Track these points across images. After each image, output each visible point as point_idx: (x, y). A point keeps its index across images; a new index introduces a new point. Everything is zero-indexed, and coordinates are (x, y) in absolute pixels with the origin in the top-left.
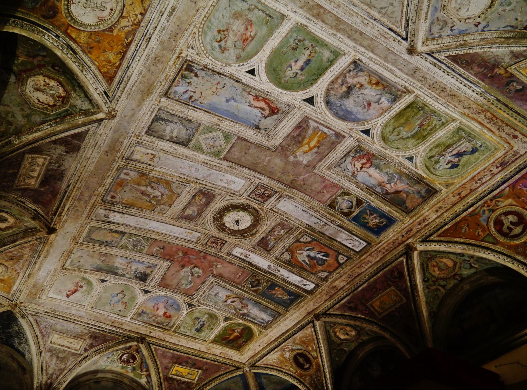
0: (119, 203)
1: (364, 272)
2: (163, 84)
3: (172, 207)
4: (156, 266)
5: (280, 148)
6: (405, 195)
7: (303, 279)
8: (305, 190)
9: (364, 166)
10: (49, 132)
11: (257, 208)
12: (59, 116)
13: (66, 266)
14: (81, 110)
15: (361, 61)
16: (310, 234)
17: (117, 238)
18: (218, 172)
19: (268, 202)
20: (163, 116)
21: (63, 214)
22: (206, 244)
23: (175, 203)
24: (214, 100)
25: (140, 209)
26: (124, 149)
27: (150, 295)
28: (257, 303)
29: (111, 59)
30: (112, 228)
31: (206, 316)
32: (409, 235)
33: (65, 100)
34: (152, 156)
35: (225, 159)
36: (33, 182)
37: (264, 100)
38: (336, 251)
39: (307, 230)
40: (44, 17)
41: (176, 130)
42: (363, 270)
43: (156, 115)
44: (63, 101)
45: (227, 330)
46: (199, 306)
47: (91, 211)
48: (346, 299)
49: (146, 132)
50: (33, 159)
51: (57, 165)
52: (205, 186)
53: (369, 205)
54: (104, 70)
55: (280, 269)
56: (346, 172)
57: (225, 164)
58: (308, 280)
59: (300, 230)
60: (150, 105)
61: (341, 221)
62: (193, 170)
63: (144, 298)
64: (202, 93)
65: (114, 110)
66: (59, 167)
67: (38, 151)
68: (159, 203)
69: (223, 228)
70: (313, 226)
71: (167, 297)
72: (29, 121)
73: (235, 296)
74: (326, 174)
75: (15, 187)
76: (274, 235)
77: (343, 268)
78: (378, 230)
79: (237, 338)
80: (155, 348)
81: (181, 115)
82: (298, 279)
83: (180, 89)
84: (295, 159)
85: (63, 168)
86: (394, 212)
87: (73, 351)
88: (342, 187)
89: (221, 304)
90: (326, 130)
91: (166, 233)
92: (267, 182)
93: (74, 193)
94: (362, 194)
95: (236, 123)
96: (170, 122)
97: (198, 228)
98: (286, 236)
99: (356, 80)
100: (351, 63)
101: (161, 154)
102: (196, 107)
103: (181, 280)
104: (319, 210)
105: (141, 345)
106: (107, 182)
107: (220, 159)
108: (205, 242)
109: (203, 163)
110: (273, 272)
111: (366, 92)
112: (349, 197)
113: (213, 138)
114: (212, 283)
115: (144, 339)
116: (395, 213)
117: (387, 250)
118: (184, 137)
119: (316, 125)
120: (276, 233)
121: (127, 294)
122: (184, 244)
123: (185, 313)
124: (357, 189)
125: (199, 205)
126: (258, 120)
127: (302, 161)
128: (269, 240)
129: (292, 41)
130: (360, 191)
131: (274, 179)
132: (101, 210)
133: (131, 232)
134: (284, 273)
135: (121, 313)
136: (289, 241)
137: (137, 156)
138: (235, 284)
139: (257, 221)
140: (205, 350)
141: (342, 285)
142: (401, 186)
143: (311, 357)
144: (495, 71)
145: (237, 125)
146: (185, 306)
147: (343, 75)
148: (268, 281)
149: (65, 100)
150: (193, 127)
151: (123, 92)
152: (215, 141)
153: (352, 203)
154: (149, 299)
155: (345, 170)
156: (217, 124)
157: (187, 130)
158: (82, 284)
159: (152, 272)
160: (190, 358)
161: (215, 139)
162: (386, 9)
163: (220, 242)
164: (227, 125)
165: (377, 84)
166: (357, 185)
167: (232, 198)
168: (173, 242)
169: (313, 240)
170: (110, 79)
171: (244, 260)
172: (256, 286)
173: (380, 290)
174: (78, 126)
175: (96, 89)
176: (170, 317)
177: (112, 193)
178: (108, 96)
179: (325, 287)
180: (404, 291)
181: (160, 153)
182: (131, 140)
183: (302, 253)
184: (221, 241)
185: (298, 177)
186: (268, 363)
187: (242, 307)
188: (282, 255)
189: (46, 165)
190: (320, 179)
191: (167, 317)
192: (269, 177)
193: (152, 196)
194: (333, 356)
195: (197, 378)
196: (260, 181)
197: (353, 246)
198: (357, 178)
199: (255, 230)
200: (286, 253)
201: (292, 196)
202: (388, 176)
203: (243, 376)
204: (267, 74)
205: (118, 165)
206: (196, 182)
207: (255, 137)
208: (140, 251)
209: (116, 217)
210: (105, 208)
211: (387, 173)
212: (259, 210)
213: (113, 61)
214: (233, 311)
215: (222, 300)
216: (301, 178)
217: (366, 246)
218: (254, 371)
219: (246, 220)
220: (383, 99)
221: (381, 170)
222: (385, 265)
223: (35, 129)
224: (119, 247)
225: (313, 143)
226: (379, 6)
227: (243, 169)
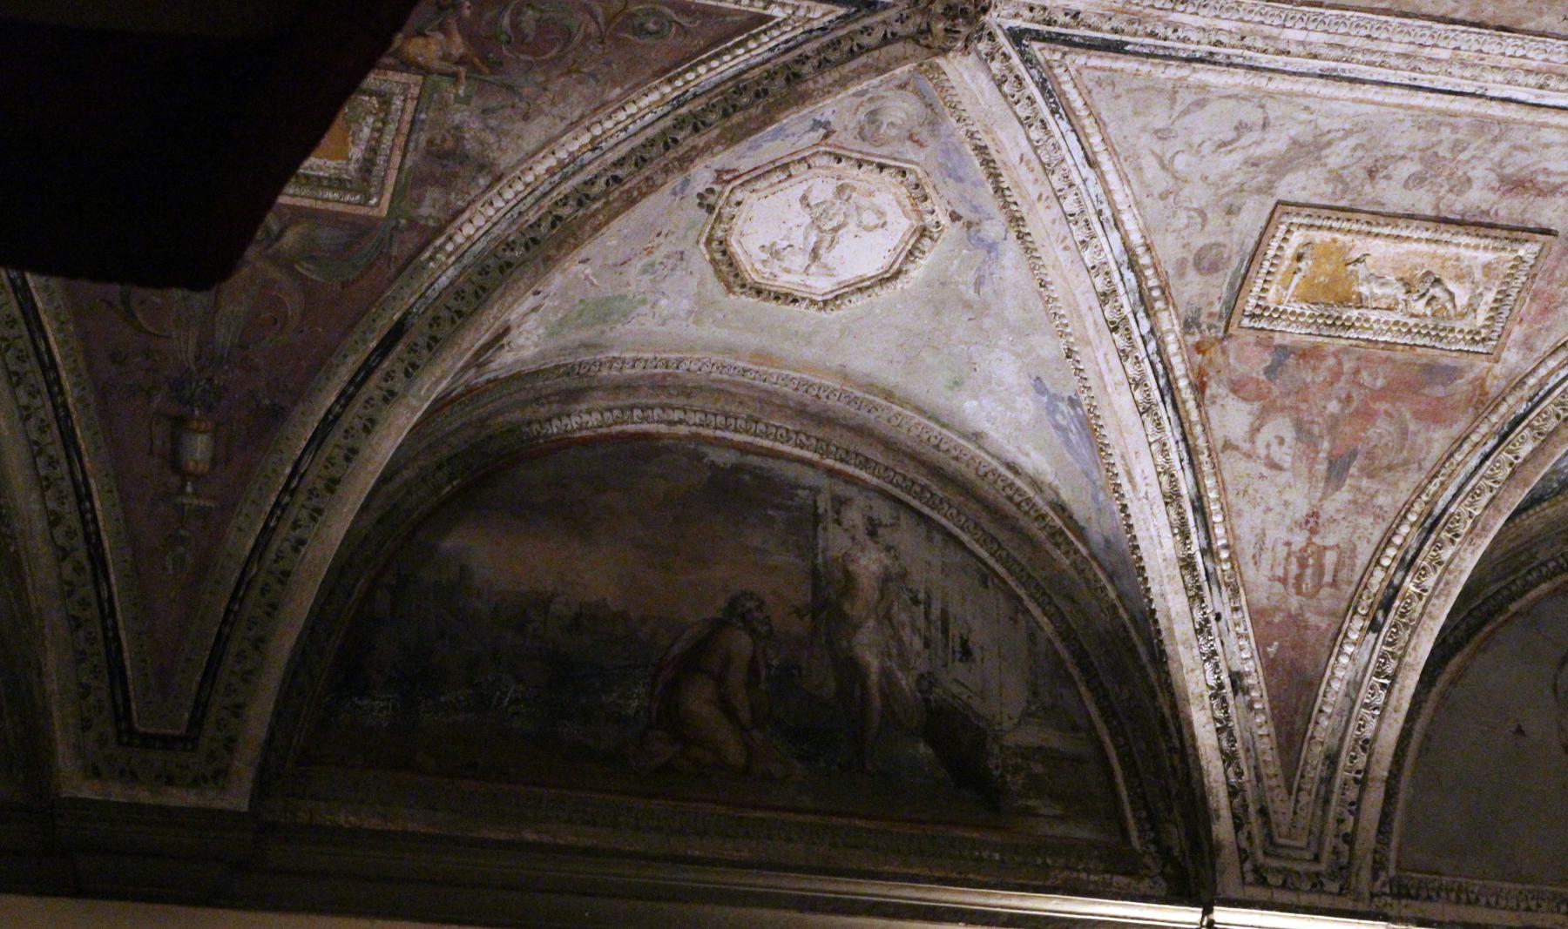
144: (458, 39)
162: (1178, 108)
226: (1215, 107)
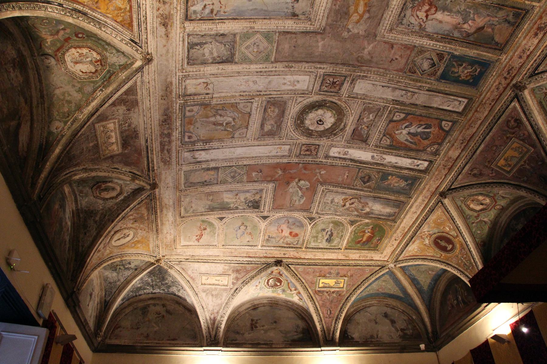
0: (198, 141)
1: (475, 132)
2: (179, 8)
3: (249, 128)
4: (261, 190)
5: (328, 27)
6: (490, 30)
7: (413, 160)
8: (376, 63)
9: (429, 13)
10: (102, 97)
11: (334, 100)
12: (105, 79)
13: (182, 215)
14: (120, 66)
16: (402, 110)
17: (213, 175)
18: (276, 77)
19: (343, 90)
20: (196, 40)
21: (155, 168)
22: (300, 154)
23: (250, 123)
24: (236, 4)
25: (220, 140)
26: (176, 88)
27: (269, 220)
29: (121, 6)
30: (203, 167)
31: (331, 225)
32: (512, 73)
33: (102, 62)
34: (205, 85)
35: (276, 61)
36: (115, 147)
38: (437, 119)
39: (396, 106)
41: (215, 50)
42: (474, 130)
43: (188, 43)
44: (101, 64)
45: (357, 233)
46: (320, 217)
47: (177, 157)
48: (467, 167)
49: (188, 63)
50: (104, 127)
51: (127, 125)
52: (270, 96)
53: (453, 56)
54: (119, 19)
55: (384, 156)
56: (411, 27)
57: (280, 67)
58: (419, 159)
59: (389, 109)
60: (178, 35)
61: (428, 84)
62: (251, 84)
63: (265, 224)
64: (220, 2)
65: (148, 54)
66: (129, 126)
67: (103, 118)
68: (235, 129)
69: (309, 133)
70: (401, 99)
71: (286, 217)
72: (83, 93)
73: (351, 197)
74: (390, 38)
76: (365, 123)
78: (474, 81)
79: (370, 239)
80: (295, 268)
81: (212, 33)
82: (409, 161)
84: (350, 33)
85: (133, 126)
86: (485, 54)
87: (223, 287)
88: (415, 46)
89: (341, 210)
91: (255, 155)
92: (331, 69)
93: (154, 145)
94: (440, 46)
95: (270, 19)
96: (205, 43)
97: (284, 140)
98: (376, 120)
101: (213, 79)
102: (222, 19)
104: (400, 80)
105: (280, 268)
106: (178, 125)
107: (272, 62)
108: (298, 152)
109: (257, 72)
110: (379, 162)
112: (427, 55)
113: (255, 44)
114: (323, 191)
115: (281, 261)
116: (487, 55)
117: (493, 100)
118: (226, 53)
120: (365, 120)
122: (278, 161)
123: (309, 227)
124: (432, 43)
125: (275, 117)
126: (291, 7)
127: (359, 33)
128: (361, 129)
130: (436, 43)
131: (338, 64)
132: (185, 153)
133: (223, 165)
134: (391, 159)
135: (251, 244)
136: (382, 124)
137: (191, 90)
138: (346, 186)
139: (340, 113)
140: (343, 258)
141: (457, 153)
142: (480, 21)
143: (451, 237)
145: (272, 20)
149: (102, 62)
150: (229, 40)
151: (147, 33)
152: (258, 46)
153: (432, 59)
154: (270, 224)
155: (409, 25)
156: (251, 28)
157: (225, 45)
158: (204, 227)
159: (261, 197)
161: (257, 44)
163: (313, 148)
164: (261, 26)
166: (429, 37)
167: (303, 99)
168: (268, 162)
170: (130, 26)
171: (345, 159)
172: (368, 181)
173: (500, 146)
174: (125, 82)
175: (122, 40)
176: (296, 235)
177: (187, 134)
178: (136, 43)
179: (439, 161)
180: (527, 139)
181: (211, 79)
182: (177, 77)
183: (401, 133)
185: (361, 53)
186: (410, 254)
188: (381, 141)
189: (117, 128)
190: (386, 46)
191: (294, 236)
192: (331, 63)
193: (225, 124)
194: (474, 230)
195: (345, 285)
196: (324, 71)
197: (453, 107)
198: (427, 30)
199: (343, 124)
200: (384, 137)
201: (365, 75)
202: (462, 15)
203: (391, 273)
205: (178, 105)
206: (260, 95)
207: (296, 25)
209: (202, 156)
210: (188, 150)
211: (458, 12)
212: (337, 101)
213: (122, 7)
214: (356, 213)
215: (340, 205)
216: (366, 51)
217: (468, 103)
218: (399, 265)
219: (329, 119)
221: (450, 11)
222: (497, 117)
223: (91, 99)
224: (219, 183)
225: (361, 9)
227: (300, 64)
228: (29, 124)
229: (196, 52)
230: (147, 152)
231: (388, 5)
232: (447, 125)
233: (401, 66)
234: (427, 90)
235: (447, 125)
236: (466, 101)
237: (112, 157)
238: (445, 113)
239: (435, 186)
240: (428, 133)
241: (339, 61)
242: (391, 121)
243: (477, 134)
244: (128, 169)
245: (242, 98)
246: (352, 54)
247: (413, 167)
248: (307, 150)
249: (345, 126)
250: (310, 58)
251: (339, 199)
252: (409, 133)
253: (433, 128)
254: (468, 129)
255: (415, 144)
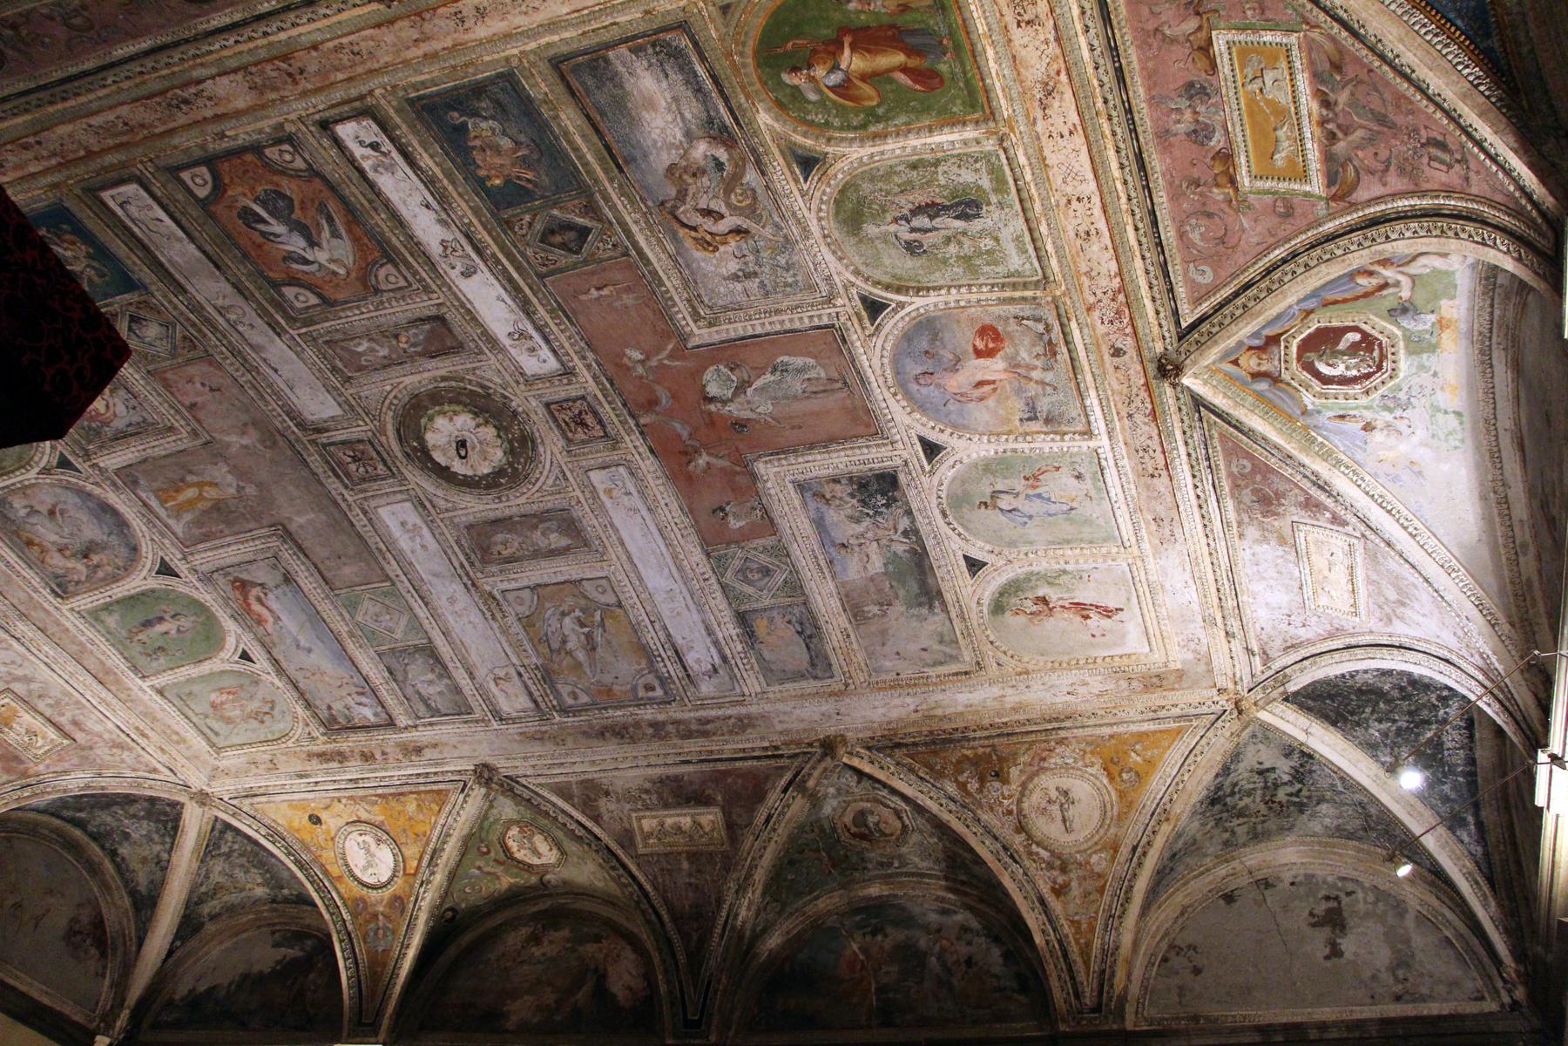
3: (575, 577)
5: (265, 522)
7: (371, 175)
8: (247, 411)
15: (53, 591)
19: (355, 436)
20: (422, 710)
21: (766, 744)
23: (561, 579)
28: (620, 159)
31: (871, 229)
35: (388, 578)
37: (249, 610)
38: (212, 216)
40: (403, 911)
42: (124, 111)
52: (466, 564)
55: (435, 249)
58: (352, 161)
59: (303, 330)
62: (458, 607)
66: (647, 792)
73: (682, 232)
75: (726, 847)
76: (390, 348)
77: (203, 147)
82: (385, 182)
83: (368, 713)
89: (768, 231)
90: (154, 503)
99: (70, 565)
100: (75, 594)
103: (795, 397)
110: (469, 249)
111: (54, 538)
119: (171, 522)
120: (384, 352)
121: (988, 490)
128: (414, 345)
129: (162, 660)
134: (428, 229)
136: (358, 317)
137: (523, 702)
139: (413, 415)
141: (223, 86)
146: (893, 324)
147: (94, 581)
148: (508, 224)
160: (1163, 135)
165: (30, 543)
169: (276, 285)
172: (570, 227)
177: (641, 693)
179: (297, 110)
183: (332, 261)
184: (560, 416)
187: (698, 173)
190: (201, 415)
193: (586, 630)
204: (223, 639)
208: (781, 552)
217: (104, 188)
220: (22, 513)
225: (191, 493)
228: (629, 954)
229: (440, 703)
230: (716, 760)
231: (145, 460)
232: (198, 181)
233: (205, 368)
234: (185, 291)
235: (198, 181)
236: (106, 195)
237: (730, 826)
238: (177, 215)
239: (388, 36)
240: (264, 204)
241: (305, 473)
242: (326, 302)
243: (122, 98)
244: (773, 797)
245: (498, 615)
246: (272, 461)
247: (395, 154)
248: (583, 424)
249: (444, 379)
250: (340, 521)
251: (719, 265)
252: (313, 243)
253: (239, 205)
254: (142, 126)
255: (322, 209)
